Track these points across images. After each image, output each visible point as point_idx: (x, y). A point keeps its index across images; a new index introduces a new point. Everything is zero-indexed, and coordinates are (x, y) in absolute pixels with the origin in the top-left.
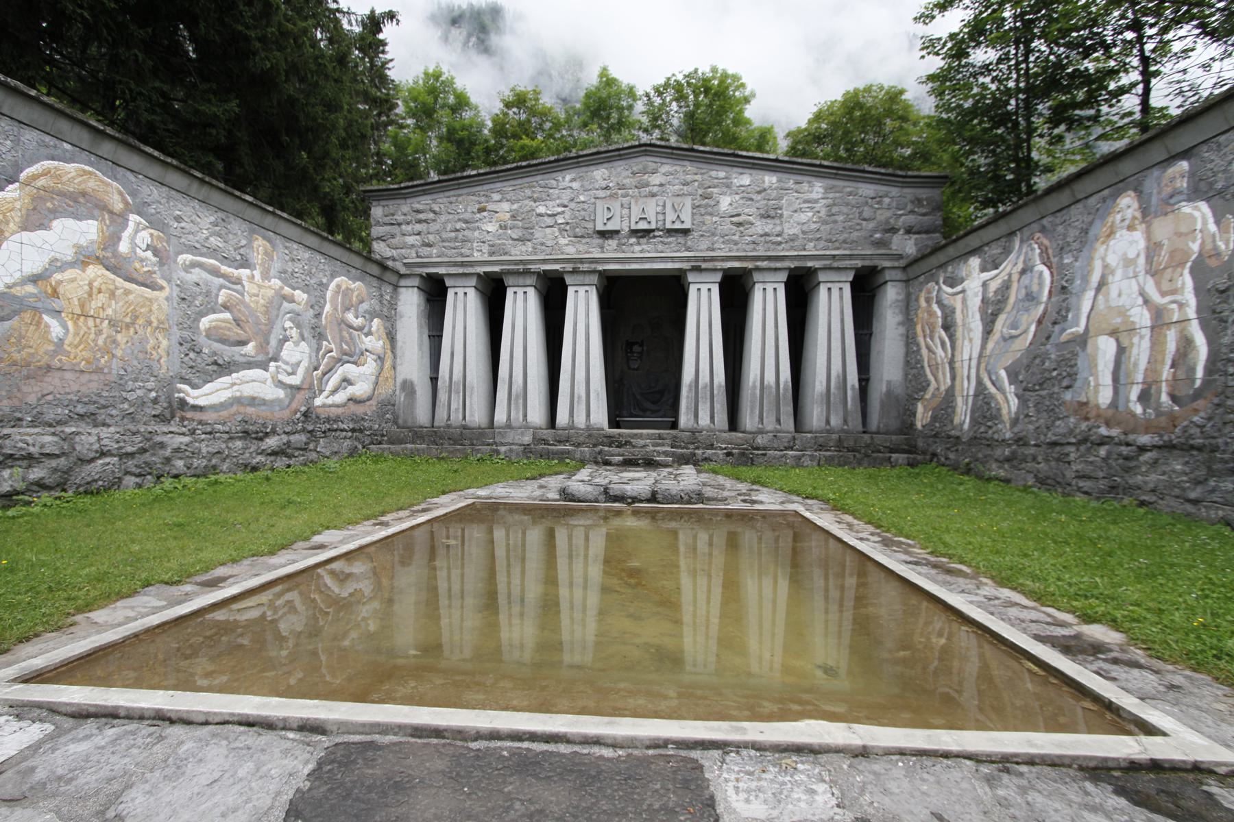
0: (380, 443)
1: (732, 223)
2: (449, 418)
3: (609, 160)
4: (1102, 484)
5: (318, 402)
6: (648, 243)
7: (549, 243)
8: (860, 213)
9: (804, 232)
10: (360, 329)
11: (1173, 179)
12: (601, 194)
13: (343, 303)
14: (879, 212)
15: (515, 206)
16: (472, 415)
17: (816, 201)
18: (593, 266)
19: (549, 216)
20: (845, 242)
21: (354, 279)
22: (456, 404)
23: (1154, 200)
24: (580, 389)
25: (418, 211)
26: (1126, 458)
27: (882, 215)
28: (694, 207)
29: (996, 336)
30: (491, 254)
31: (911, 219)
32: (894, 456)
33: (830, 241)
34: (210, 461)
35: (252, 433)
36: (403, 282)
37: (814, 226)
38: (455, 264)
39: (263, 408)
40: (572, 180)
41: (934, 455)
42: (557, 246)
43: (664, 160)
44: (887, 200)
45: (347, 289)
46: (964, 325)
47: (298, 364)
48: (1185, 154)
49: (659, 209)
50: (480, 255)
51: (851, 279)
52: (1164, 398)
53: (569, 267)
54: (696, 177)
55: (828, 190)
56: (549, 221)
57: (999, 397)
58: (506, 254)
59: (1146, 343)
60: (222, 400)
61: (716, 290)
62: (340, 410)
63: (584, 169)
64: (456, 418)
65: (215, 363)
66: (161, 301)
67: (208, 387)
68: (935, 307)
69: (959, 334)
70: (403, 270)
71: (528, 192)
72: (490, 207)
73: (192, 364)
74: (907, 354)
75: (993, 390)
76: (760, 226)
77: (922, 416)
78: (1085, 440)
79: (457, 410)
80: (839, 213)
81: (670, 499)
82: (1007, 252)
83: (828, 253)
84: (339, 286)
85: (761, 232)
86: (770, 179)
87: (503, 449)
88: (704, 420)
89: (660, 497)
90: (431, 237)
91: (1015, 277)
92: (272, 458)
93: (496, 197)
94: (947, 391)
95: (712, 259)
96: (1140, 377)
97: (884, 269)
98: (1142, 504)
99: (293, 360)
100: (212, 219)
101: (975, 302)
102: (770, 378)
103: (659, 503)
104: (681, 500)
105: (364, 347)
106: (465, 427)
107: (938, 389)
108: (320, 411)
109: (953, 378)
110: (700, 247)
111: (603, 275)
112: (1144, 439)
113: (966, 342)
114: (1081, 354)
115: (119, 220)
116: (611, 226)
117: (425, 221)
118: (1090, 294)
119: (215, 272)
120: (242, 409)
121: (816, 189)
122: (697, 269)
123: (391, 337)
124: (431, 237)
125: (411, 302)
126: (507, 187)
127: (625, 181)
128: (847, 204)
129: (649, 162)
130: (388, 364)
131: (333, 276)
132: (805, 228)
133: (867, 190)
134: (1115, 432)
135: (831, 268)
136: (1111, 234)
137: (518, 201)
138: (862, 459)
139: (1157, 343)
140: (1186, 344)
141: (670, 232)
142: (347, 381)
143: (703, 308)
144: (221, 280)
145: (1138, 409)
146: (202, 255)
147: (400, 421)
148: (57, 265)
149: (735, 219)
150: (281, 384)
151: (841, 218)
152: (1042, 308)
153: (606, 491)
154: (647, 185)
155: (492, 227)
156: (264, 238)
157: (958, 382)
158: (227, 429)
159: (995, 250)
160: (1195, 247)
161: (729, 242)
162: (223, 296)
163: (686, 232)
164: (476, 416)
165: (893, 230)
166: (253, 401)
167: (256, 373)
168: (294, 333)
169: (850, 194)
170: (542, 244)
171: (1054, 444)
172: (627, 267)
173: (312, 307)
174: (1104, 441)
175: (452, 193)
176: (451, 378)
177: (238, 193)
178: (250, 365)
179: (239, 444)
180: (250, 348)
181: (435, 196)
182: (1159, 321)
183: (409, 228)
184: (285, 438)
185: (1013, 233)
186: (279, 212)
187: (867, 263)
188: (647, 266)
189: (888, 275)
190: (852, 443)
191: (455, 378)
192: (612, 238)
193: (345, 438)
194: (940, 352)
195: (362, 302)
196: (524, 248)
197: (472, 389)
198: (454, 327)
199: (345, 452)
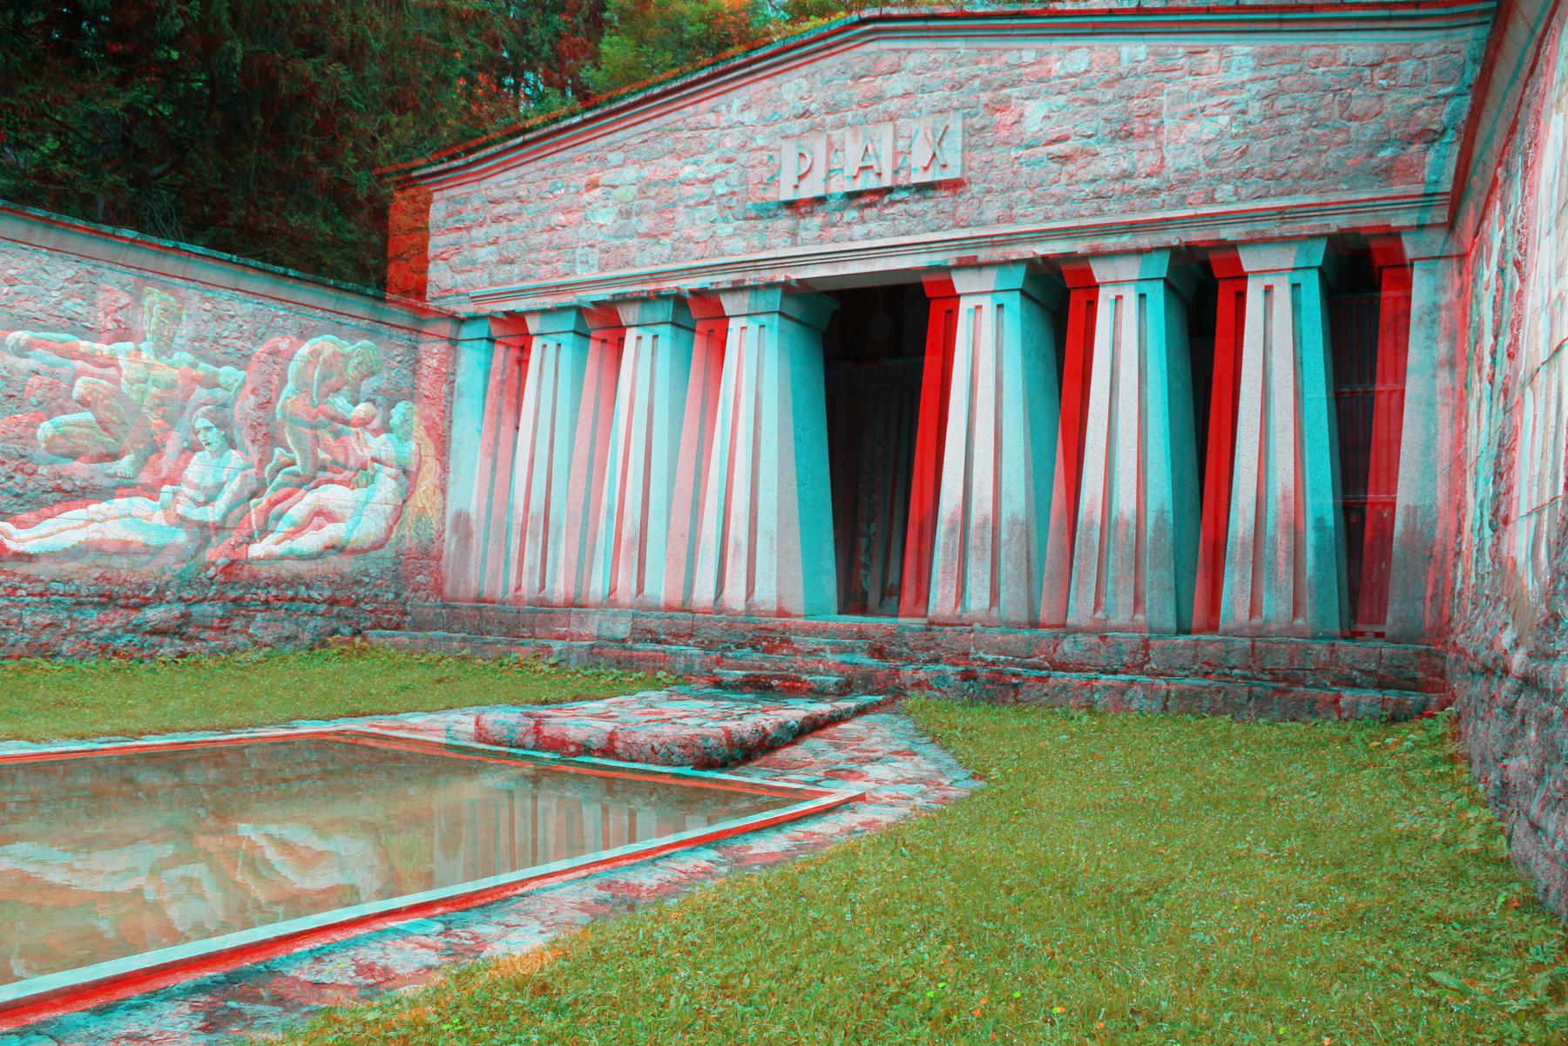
0: (398, 627)
1: (1053, 158)
3: (811, 57)
5: (256, 550)
6: (880, 217)
7: (699, 235)
8: (1345, 105)
9: (1211, 162)
10: (364, 423)
12: (795, 127)
13: (323, 378)
14: (1393, 95)
15: (645, 172)
18: (767, 276)
19: (703, 182)
20: (1307, 174)
21: (352, 338)
22: (531, 558)
24: (739, 530)
25: (495, 202)
27: (1398, 103)
32: (1348, 695)
33: (1274, 177)
34: (37, 636)
36: (466, 332)
37: (1232, 146)
39: (145, 558)
40: (746, 107)
42: (712, 242)
43: (914, 44)
44: (1408, 66)
45: (335, 354)
47: (219, 487)
49: (901, 144)
50: (589, 274)
51: (1318, 262)
53: (724, 280)
54: (975, 70)
55: (1262, 61)
56: (702, 192)
60: (68, 545)
61: (1157, 293)
62: (303, 567)
63: (766, 83)
65: (58, 489)
67: (46, 526)
71: (668, 141)
72: (607, 177)
73: (18, 490)
76: (1110, 160)
79: (532, 568)
80: (1292, 109)
81: (634, 753)
83: (1264, 204)
84: (316, 353)
85: (1113, 171)
86: (1133, 51)
87: (557, 646)
92: (155, 639)
93: (615, 158)
95: (1011, 239)
99: (209, 481)
100: (70, 273)
102: (1125, 502)
103: (618, 758)
104: (653, 755)
105: (367, 454)
106: (543, 603)
108: (256, 567)
110: (986, 215)
111: (787, 288)
116: (808, 190)
120: (103, 561)
121: (1236, 61)
126: (630, 135)
127: (838, 97)
128: (1313, 88)
129: (881, 50)
130: (427, 482)
131: (303, 335)
132: (1212, 151)
133: (1359, 47)
135: (1267, 241)
137: (649, 161)
138: (1268, 699)
141: (922, 188)
142: (323, 515)
143: (988, 349)
144: (79, 364)
146: (47, 329)
147: (447, 589)
149: (1054, 149)
150: (182, 520)
151: (1294, 121)
154: (880, 98)
156: (164, 289)
158: (71, 589)
162: (79, 389)
163: (955, 185)
166: (124, 548)
167: (139, 504)
168: (214, 436)
169: (1319, 61)
170: (688, 239)
172: (841, 270)
173: (253, 391)
176: (527, 508)
177: (107, 229)
179: (93, 614)
180: (124, 465)
181: (523, 170)
184: (178, 609)
186: (183, 246)
187: (1364, 220)
190: (1283, 662)
191: (533, 506)
192: (811, 213)
193: (313, 613)
195: (372, 374)
196: (657, 250)
197: (559, 527)
198: (537, 412)
199: (306, 637)
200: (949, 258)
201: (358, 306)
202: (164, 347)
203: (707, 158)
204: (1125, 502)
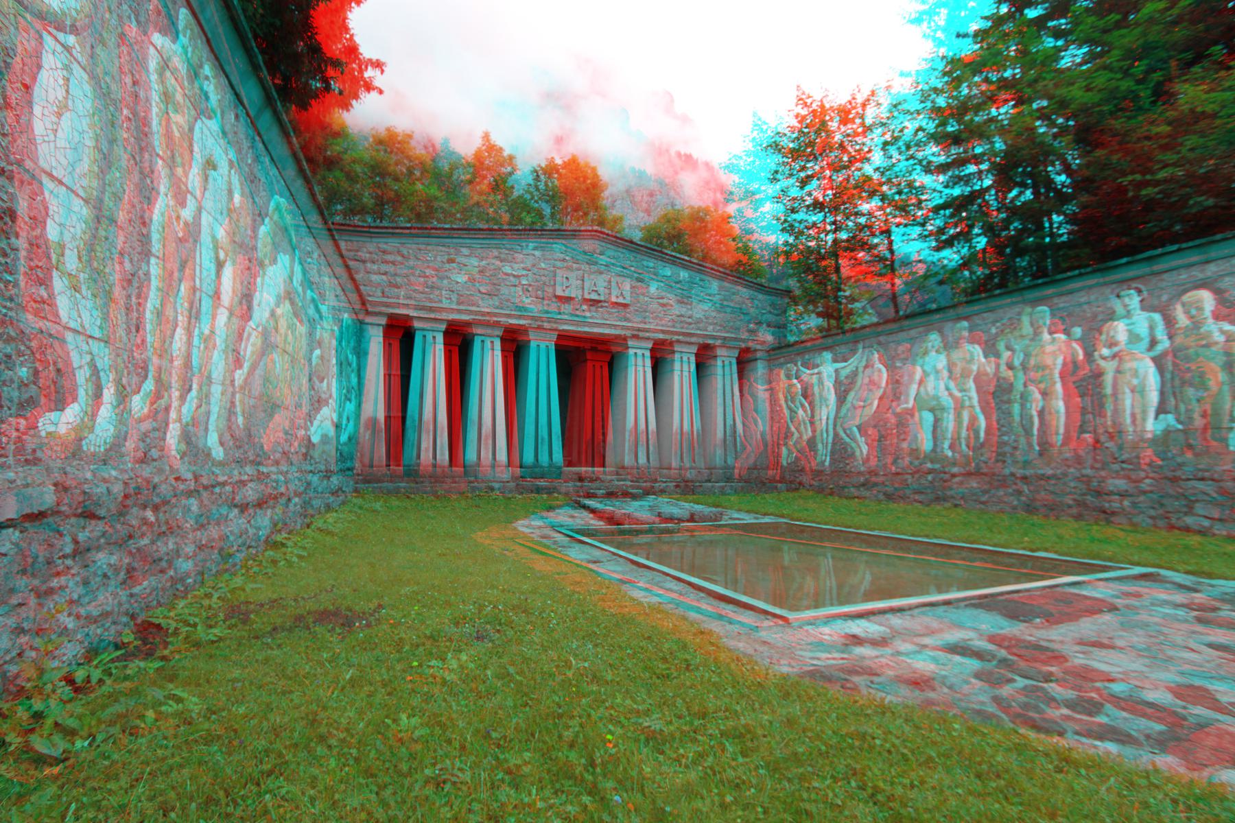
2: (419, 456)
3: (565, 237)
4: (931, 496)
11: (960, 330)
12: (559, 264)
15: (483, 263)
16: (442, 454)
17: (714, 295)
18: (555, 326)
23: (950, 339)
24: (543, 432)
25: (384, 252)
26: (945, 481)
28: (632, 287)
29: (848, 405)
30: (459, 303)
31: (770, 318)
36: (369, 319)
38: (423, 308)
40: (535, 249)
41: (800, 483)
46: (821, 396)
48: (966, 318)
52: (964, 447)
55: (720, 288)
57: (853, 445)
58: (473, 305)
59: (951, 417)
68: (795, 381)
69: (817, 402)
71: (496, 253)
72: (459, 259)
74: (772, 411)
75: (848, 440)
76: (677, 310)
77: (786, 456)
78: (918, 472)
79: (427, 449)
82: (854, 352)
86: (684, 274)
88: (642, 460)
89: (696, 517)
90: (399, 279)
91: (860, 370)
93: (465, 251)
94: (809, 440)
96: (949, 436)
97: (756, 350)
98: (956, 506)
101: (829, 384)
102: (686, 427)
107: (801, 437)
109: (814, 431)
112: (955, 470)
113: (824, 408)
114: (911, 422)
116: (567, 294)
117: (393, 263)
118: (914, 387)
122: (635, 337)
124: (399, 279)
134: (937, 466)
136: (926, 353)
139: (958, 417)
140: (973, 419)
145: (950, 454)
152: (881, 391)
153: (659, 515)
154: (596, 263)
155: (462, 279)
157: (818, 432)
159: (843, 350)
160: (975, 368)
161: (656, 318)
163: (625, 306)
165: (760, 323)
170: (508, 300)
171: (898, 474)
174: (930, 471)
175: (421, 240)
181: (403, 240)
182: (959, 406)
183: (375, 267)
185: (856, 342)
188: (595, 330)
189: (759, 355)
194: (801, 412)
200: (628, 333)
203: (516, 266)
204: (686, 427)
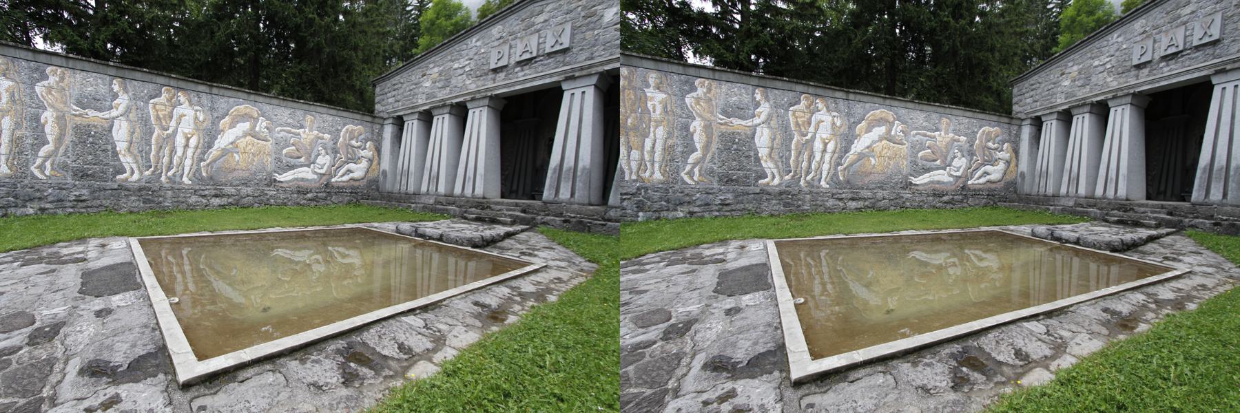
35: (301, 191)
64: (403, 188)
66: (269, 145)
70: (386, 116)
115: (256, 120)
119: (290, 132)
123: (378, 150)
125: (389, 130)
130: (375, 162)
142: (349, 171)
148: (238, 138)
164: (411, 189)
166: (303, 179)
178: (302, 166)
201: (358, 117)
202: (311, 130)
